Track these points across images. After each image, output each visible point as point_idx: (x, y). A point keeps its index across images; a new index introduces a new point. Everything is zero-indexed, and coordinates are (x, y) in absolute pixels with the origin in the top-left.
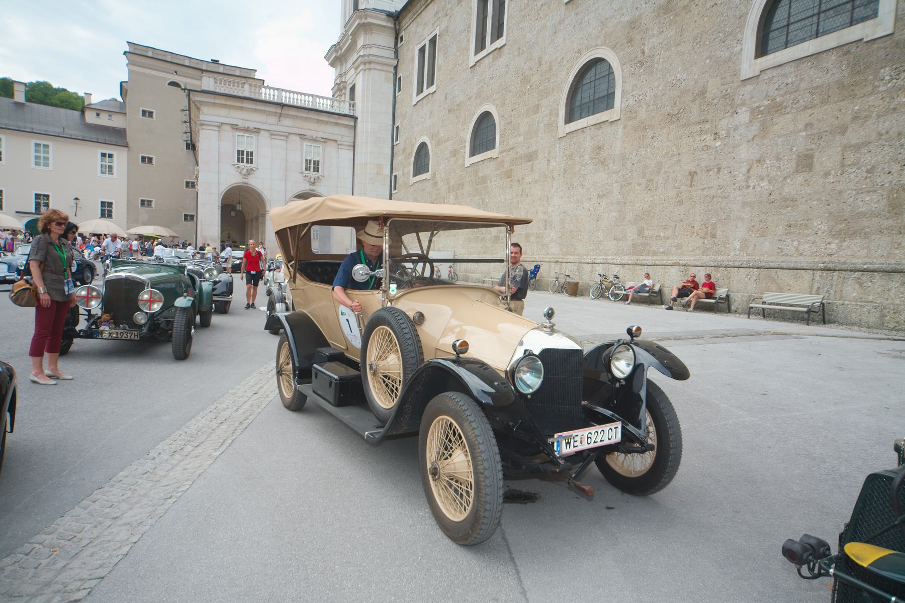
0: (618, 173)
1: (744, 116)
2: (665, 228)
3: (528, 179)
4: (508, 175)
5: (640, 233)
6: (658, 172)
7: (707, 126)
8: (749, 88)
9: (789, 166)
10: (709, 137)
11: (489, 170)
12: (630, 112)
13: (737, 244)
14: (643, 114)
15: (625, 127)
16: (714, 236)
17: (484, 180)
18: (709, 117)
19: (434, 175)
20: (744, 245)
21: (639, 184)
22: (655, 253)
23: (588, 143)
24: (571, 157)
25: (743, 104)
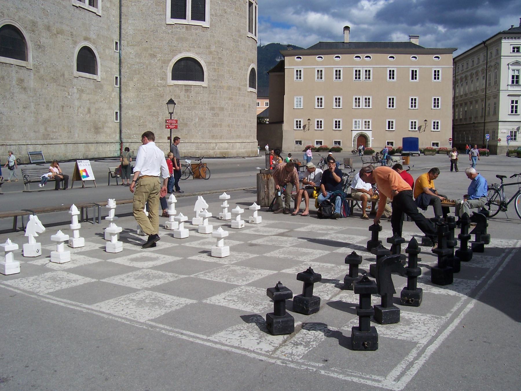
0: (33, 97)
1: (75, 90)
2: (55, 128)
6: (51, 102)
7: (66, 89)
8: (76, 80)
9: (86, 110)
10: (67, 94)
13: (77, 135)
15: (35, 75)
16: (71, 132)
18: (66, 85)
20: (78, 136)
21: (43, 106)
22: (52, 139)
25: (75, 85)
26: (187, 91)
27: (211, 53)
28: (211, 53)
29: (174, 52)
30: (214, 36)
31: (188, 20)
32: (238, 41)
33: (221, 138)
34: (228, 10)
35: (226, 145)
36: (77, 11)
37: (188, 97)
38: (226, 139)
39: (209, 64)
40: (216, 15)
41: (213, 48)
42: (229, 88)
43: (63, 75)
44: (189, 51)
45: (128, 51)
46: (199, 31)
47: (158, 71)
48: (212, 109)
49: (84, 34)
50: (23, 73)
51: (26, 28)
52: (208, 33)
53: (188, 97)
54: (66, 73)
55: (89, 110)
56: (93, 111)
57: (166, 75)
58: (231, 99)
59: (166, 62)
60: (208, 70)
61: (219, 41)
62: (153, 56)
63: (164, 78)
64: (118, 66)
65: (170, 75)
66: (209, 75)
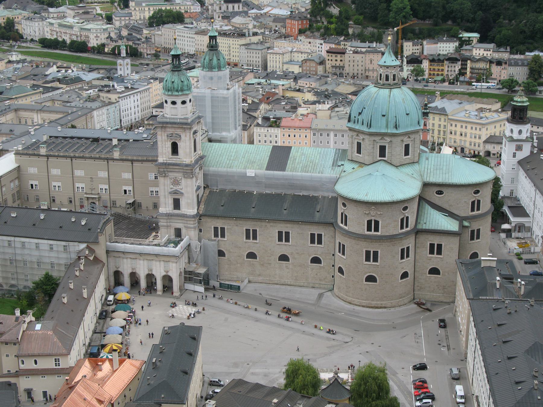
4: (263, 265)
23: (284, 265)
55: (317, 274)
56: (319, 274)
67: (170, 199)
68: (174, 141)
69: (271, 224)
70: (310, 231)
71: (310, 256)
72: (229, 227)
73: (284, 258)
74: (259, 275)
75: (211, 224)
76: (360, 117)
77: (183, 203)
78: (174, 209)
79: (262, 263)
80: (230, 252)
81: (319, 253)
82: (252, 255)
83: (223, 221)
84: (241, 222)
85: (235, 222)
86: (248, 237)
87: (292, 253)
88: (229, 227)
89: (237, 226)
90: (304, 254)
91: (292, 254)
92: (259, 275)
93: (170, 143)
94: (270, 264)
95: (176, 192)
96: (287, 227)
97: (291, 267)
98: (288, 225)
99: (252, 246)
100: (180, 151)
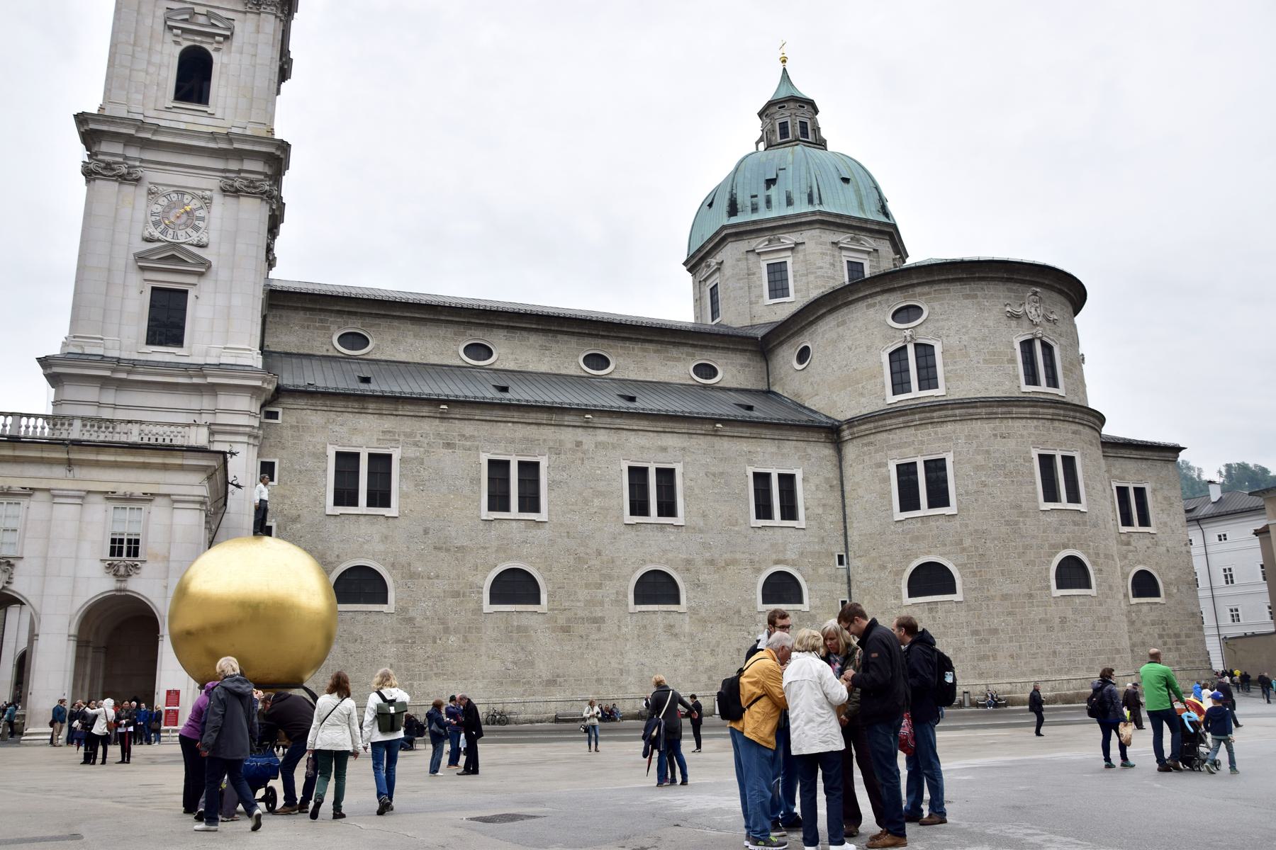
3: (593, 636)
4: (566, 630)
5: (710, 678)
11: (533, 621)
12: (693, 610)
14: (703, 613)
17: (521, 629)
19: (402, 610)
24: (645, 627)
26: (931, 610)
27: (964, 550)
28: (964, 550)
29: (908, 558)
30: (967, 526)
31: (924, 510)
32: (1017, 523)
33: (996, 676)
34: (990, 481)
35: (1008, 687)
36: (761, 532)
37: (934, 619)
38: (1009, 676)
39: (961, 567)
40: (967, 493)
41: (967, 542)
42: (1005, 597)
43: (739, 612)
44: (929, 553)
45: (856, 563)
46: (941, 522)
47: (891, 587)
48: (975, 633)
49: (774, 557)
50: (671, 619)
51: (676, 569)
52: (956, 523)
53: (934, 619)
54: (744, 611)
57: (900, 591)
58: (1009, 614)
59: (899, 573)
60: (962, 576)
61: (976, 531)
62: (883, 567)
63: (898, 597)
64: (845, 586)
65: (905, 591)
66: (964, 584)
67: (133, 292)
68: (198, 40)
69: (602, 436)
70: (750, 462)
71: (758, 571)
72: (412, 452)
73: (656, 588)
74: (552, 682)
75: (326, 436)
76: (773, 191)
77: (198, 315)
78: (150, 341)
79: (561, 620)
80: (413, 576)
81: (790, 555)
82: (515, 587)
83: (388, 423)
84: (469, 428)
85: (442, 427)
86: (498, 501)
87: (688, 562)
88: (412, 452)
89: (449, 445)
90: (734, 562)
91: (688, 565)
92: (552, 682)
93: (177, 50)
94: (598, 621)
95: (173, 257)
96: (664, 449)
97: (686, 626)
98: (671, 441)
99: (517, 540)
100: (219, 86)
